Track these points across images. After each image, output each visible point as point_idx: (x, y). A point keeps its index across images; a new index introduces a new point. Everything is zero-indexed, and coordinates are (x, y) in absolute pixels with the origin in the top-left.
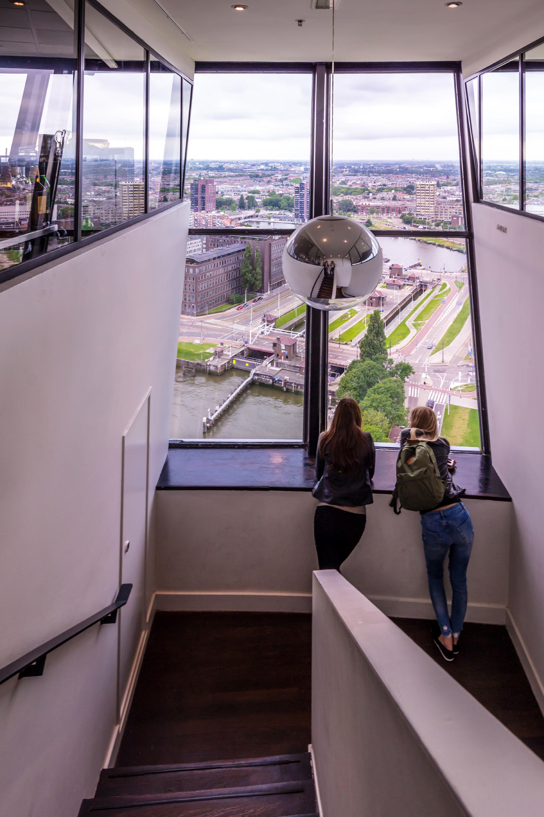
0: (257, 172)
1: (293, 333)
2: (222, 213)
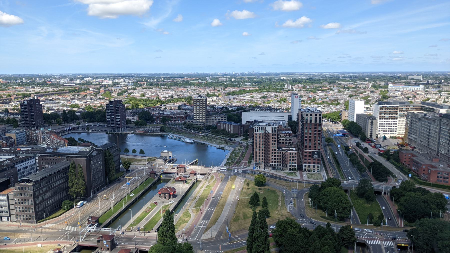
0: (76, 87)
1: (111, 230)
2: (49, 129)
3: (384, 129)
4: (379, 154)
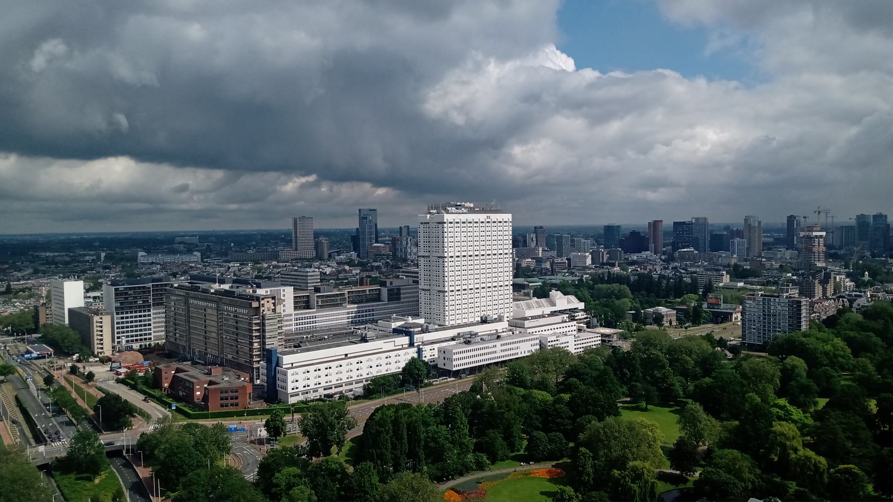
3: (127, 332)
4: (119, 381)
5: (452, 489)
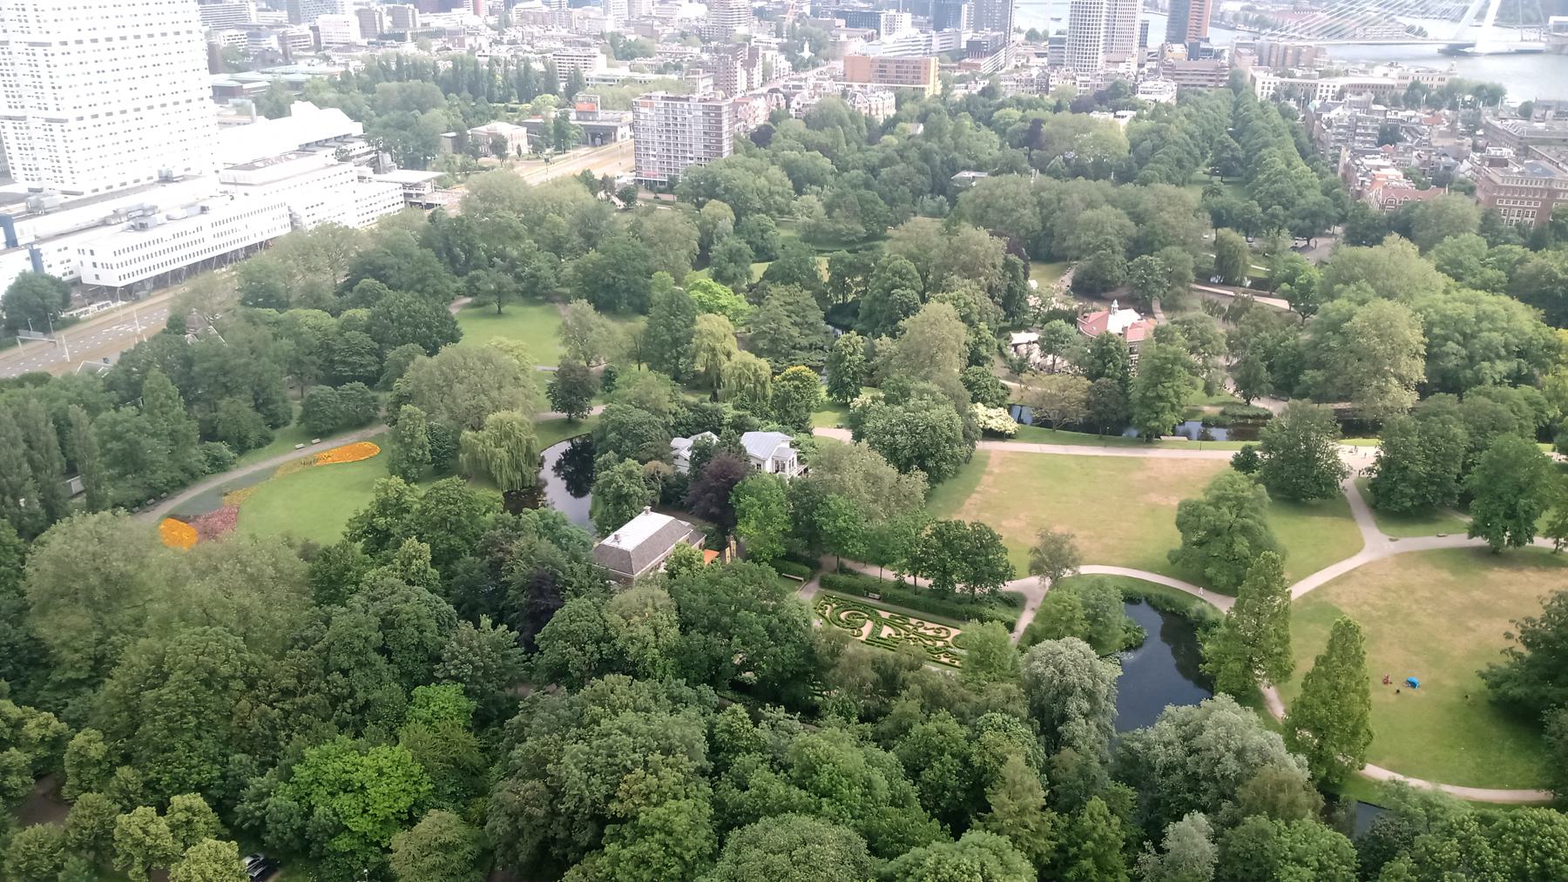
5: (173, 516)
